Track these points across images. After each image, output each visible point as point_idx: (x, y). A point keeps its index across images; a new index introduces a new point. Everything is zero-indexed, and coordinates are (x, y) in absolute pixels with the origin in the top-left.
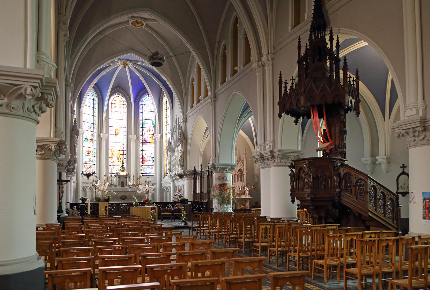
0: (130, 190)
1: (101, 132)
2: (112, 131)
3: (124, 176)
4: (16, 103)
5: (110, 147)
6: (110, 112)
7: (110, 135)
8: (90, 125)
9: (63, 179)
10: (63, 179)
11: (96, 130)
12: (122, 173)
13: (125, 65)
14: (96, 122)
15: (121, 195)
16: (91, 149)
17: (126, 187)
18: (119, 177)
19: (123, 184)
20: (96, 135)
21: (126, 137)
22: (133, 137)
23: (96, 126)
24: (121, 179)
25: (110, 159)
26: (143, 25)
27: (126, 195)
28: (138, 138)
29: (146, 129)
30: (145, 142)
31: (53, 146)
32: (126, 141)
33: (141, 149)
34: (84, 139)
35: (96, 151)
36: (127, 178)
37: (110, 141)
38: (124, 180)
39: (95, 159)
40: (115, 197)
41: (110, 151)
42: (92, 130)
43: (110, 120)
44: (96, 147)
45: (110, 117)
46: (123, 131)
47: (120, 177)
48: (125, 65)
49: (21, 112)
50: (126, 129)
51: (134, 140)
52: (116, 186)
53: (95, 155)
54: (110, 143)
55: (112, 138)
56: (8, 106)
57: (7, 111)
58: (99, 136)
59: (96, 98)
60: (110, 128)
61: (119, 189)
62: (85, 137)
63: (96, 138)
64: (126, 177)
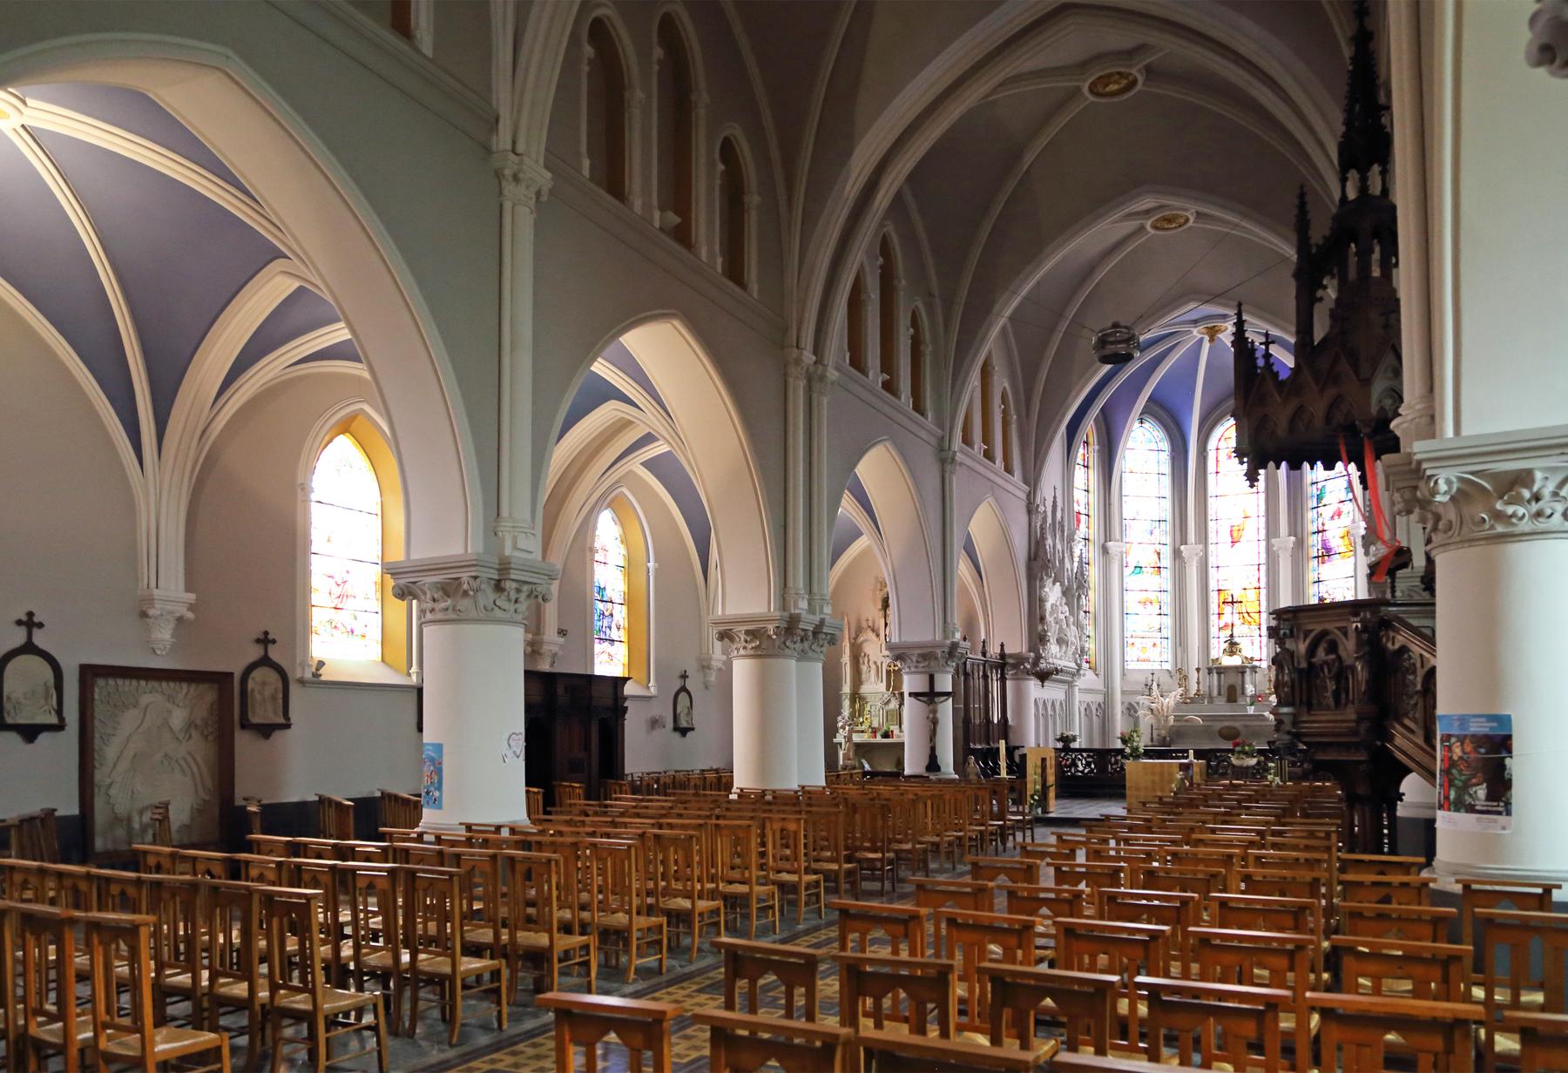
0: (1251, 710)
1: (1184, 541)
2: (1218, 532)
3: (1236, 668)
4: (464, 604)
5: (1213, 585)
6: (1211, 478)
7: (1211, 548)
8: (1148, 526)
9: (937, 689)
10: (937, 689)
11: (1168, 539)
12: (1228, 661)
13: (1213, 333)
14: (1168, 515)
15: (1218, 725)
16: (1153, 596)
17: (1241, 701)
18: (1219, 674)
19: (1233, 694)
20: (1167, 552)
21: (1263, 544)
22: (1286, 541)
23: (1167, 527)
24: (1228, 680)
25: (1213, 619)
26: (1187, 220)
27: (1237, 724)
28: (1300, 544)
29: (1327, 512)
30: (1327, 553)
31: (771, 628)
32: (1263, 559)
33: (1312, 576)
34: (1127, 571)
35: (1167, 598)
36: (1243, 673)
37: (1212, 561)
38: (1233, 679)
39: (1168, 621)
40: (1205, 732)
41: (1213, 597)
42: (1157, 537)
43: (1211, 501)
44: (1168, 586)
45: (1211, 490)
46: (1255, 529)
47: (1222, 671)
48: (1213, 333)
49: (473, 614)
50: (1263, 520)
51: (1289, 552)
52: (1211, 697)
53: (1167, 609)
54: (1212, 572)
55: (1220, 552)
56: (454, 609)
57: (453, 616)
58: (1177, 554)
59: (1165, 445)
60: (1211, 525)
61: (1222, 708)
62: (1132, 564)
63: (1167, 561)
64: (1240, 670)
